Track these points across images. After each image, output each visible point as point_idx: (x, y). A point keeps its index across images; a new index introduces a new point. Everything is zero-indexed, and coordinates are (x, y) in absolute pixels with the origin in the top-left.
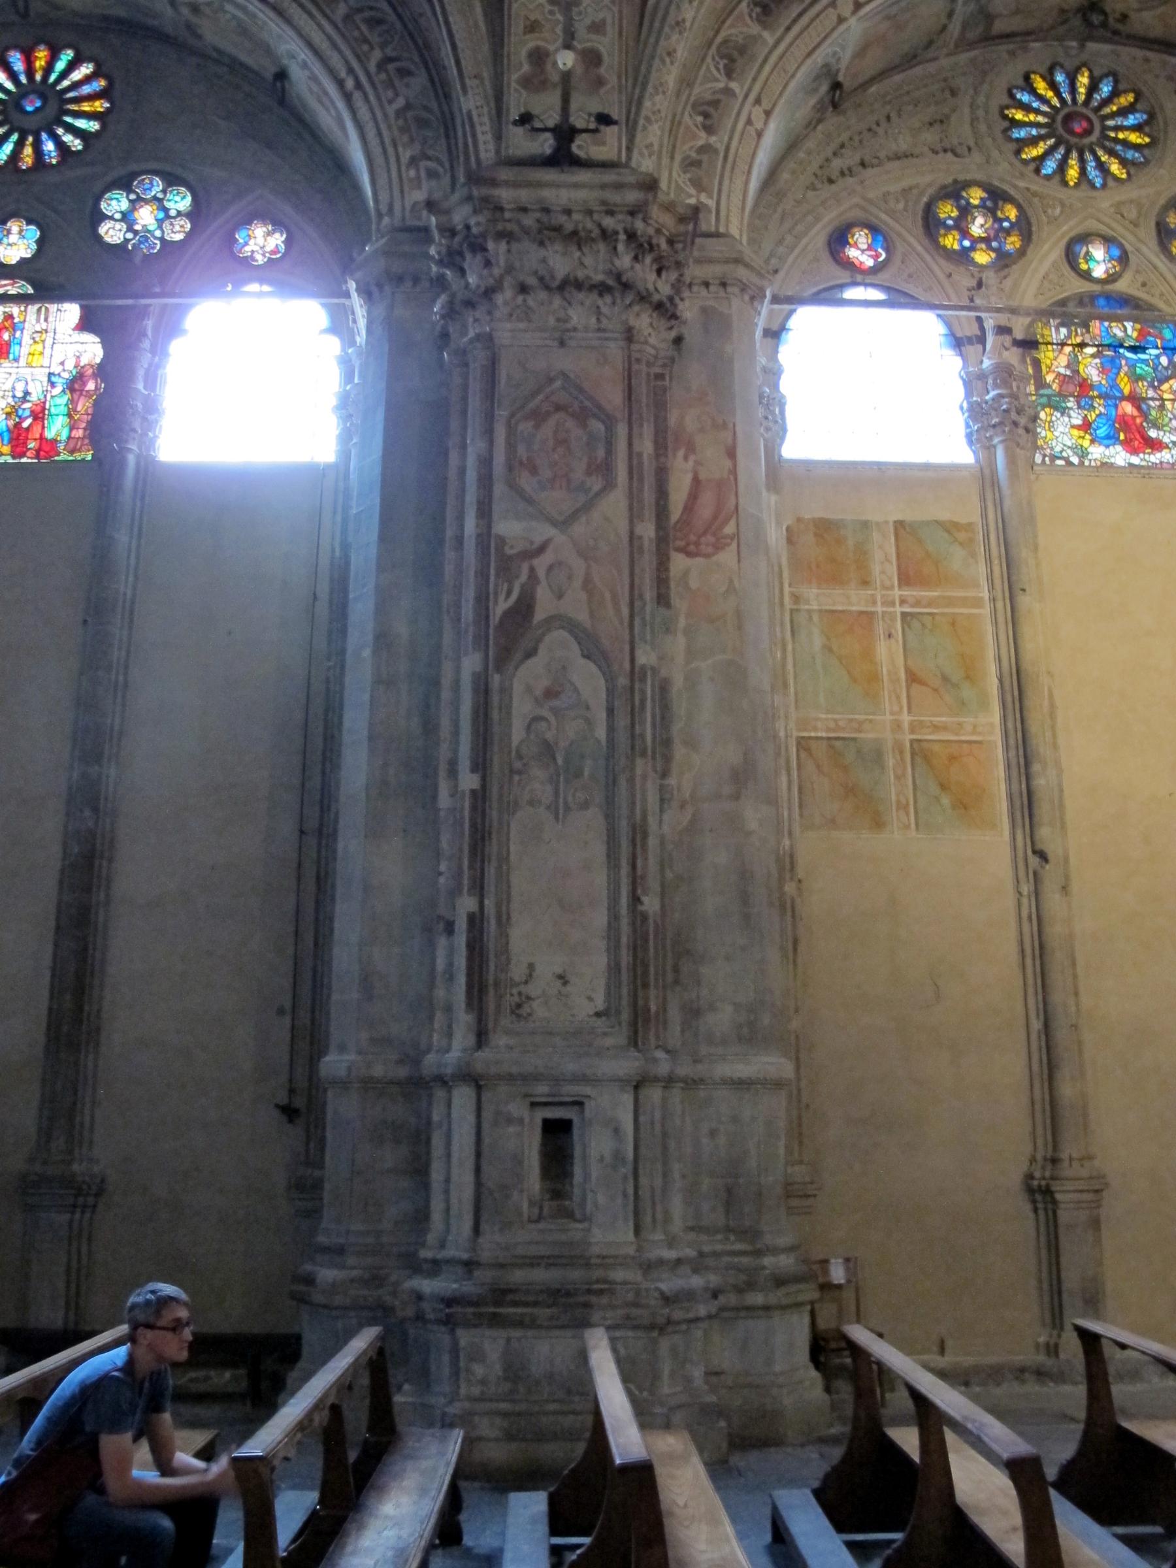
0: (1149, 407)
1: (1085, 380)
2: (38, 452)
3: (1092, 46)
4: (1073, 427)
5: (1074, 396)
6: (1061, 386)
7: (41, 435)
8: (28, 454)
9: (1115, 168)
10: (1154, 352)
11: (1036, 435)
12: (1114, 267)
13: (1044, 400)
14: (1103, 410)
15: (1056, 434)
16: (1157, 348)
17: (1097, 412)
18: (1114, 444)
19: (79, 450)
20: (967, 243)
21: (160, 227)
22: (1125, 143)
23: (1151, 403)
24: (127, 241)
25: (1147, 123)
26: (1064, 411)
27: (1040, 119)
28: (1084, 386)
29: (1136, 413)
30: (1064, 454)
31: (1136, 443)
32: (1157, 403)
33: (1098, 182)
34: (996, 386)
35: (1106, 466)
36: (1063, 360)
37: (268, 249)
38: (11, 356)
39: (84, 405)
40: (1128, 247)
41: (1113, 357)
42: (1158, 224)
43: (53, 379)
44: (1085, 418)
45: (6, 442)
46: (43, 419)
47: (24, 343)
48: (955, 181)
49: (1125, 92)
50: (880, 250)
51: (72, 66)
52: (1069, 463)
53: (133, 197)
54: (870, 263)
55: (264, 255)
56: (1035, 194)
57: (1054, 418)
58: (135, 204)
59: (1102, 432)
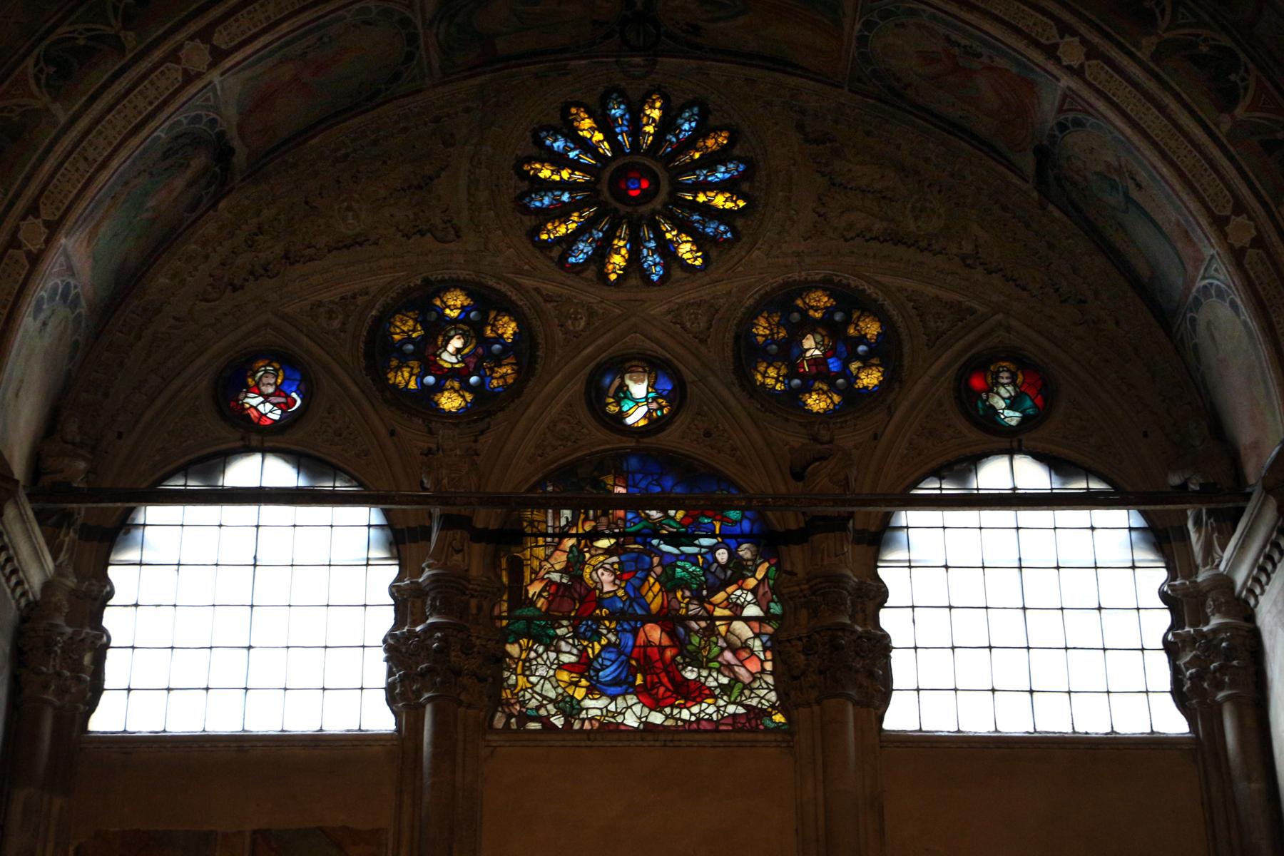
0: (689, 630)
1: (590, 591)
3: (668, 63)
4: (562, 666)
5: (568, 618)
6: (550, 603)
9: (686, 250)
10: (706, 542)
11: (500, 683)
12: (661, 408)
13: (521, 625)
14: (613, 639)
15: (533, 679)
16: (713, 536)
17: (604, 642)
18: (624, 694)
20: (430, 380)
22: (709, 211)
23: (694, 625)
25: (743, 176)
26: (551, 643)
27: (578, 176)
28: (592, 596)
29: (666, 641)
30: (543, 712)
31: (662, 689)
32: (703, 624)
33: (656, 273)
34: (435, 610)
35: (609, 729)
36: (560, 560)
40: (688, 375)
41: (639, 552)
42: (737, 337)
44: (582, 653)
48: (426, 281)
49: (717, 130)
50: (294, 395)
52: (548, 726)
54: (276, 415)
56: (548, 299)
57: (533, 655)
59: (606, 675)
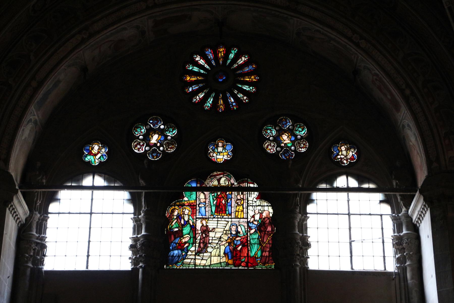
2: (247, 263)
7: (248, 254)
8: (242, 264)
19: (268, 263)
21: (293, 145)
24: (278, 152)
37: (349, 157)
38: (227, 212)
39: (267, 239)
43: (250, 225)
45: (230, 258)
46: (248, 246)
47: (233, 205)
51: (237, 57)
53: (277, 128)
55: (347, 160)
58: (280, 132)
